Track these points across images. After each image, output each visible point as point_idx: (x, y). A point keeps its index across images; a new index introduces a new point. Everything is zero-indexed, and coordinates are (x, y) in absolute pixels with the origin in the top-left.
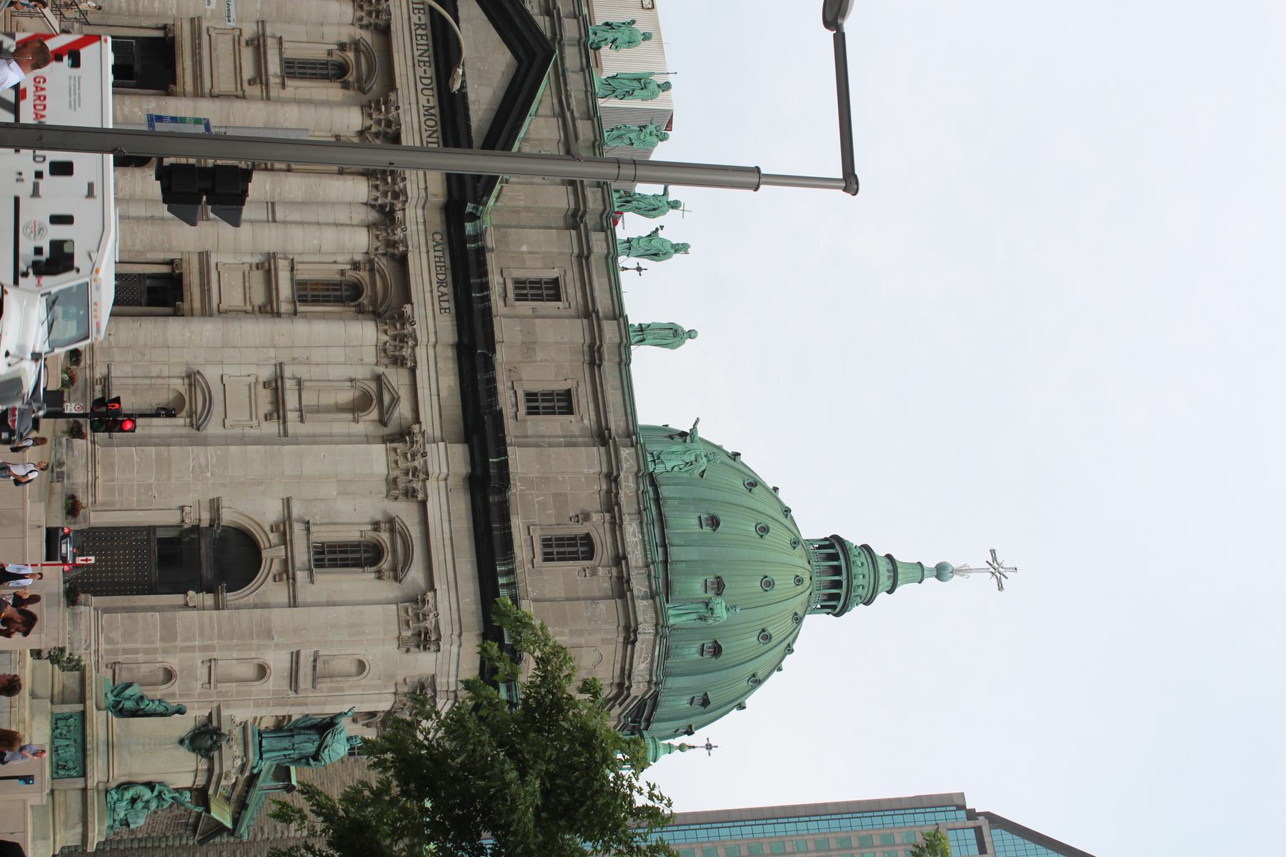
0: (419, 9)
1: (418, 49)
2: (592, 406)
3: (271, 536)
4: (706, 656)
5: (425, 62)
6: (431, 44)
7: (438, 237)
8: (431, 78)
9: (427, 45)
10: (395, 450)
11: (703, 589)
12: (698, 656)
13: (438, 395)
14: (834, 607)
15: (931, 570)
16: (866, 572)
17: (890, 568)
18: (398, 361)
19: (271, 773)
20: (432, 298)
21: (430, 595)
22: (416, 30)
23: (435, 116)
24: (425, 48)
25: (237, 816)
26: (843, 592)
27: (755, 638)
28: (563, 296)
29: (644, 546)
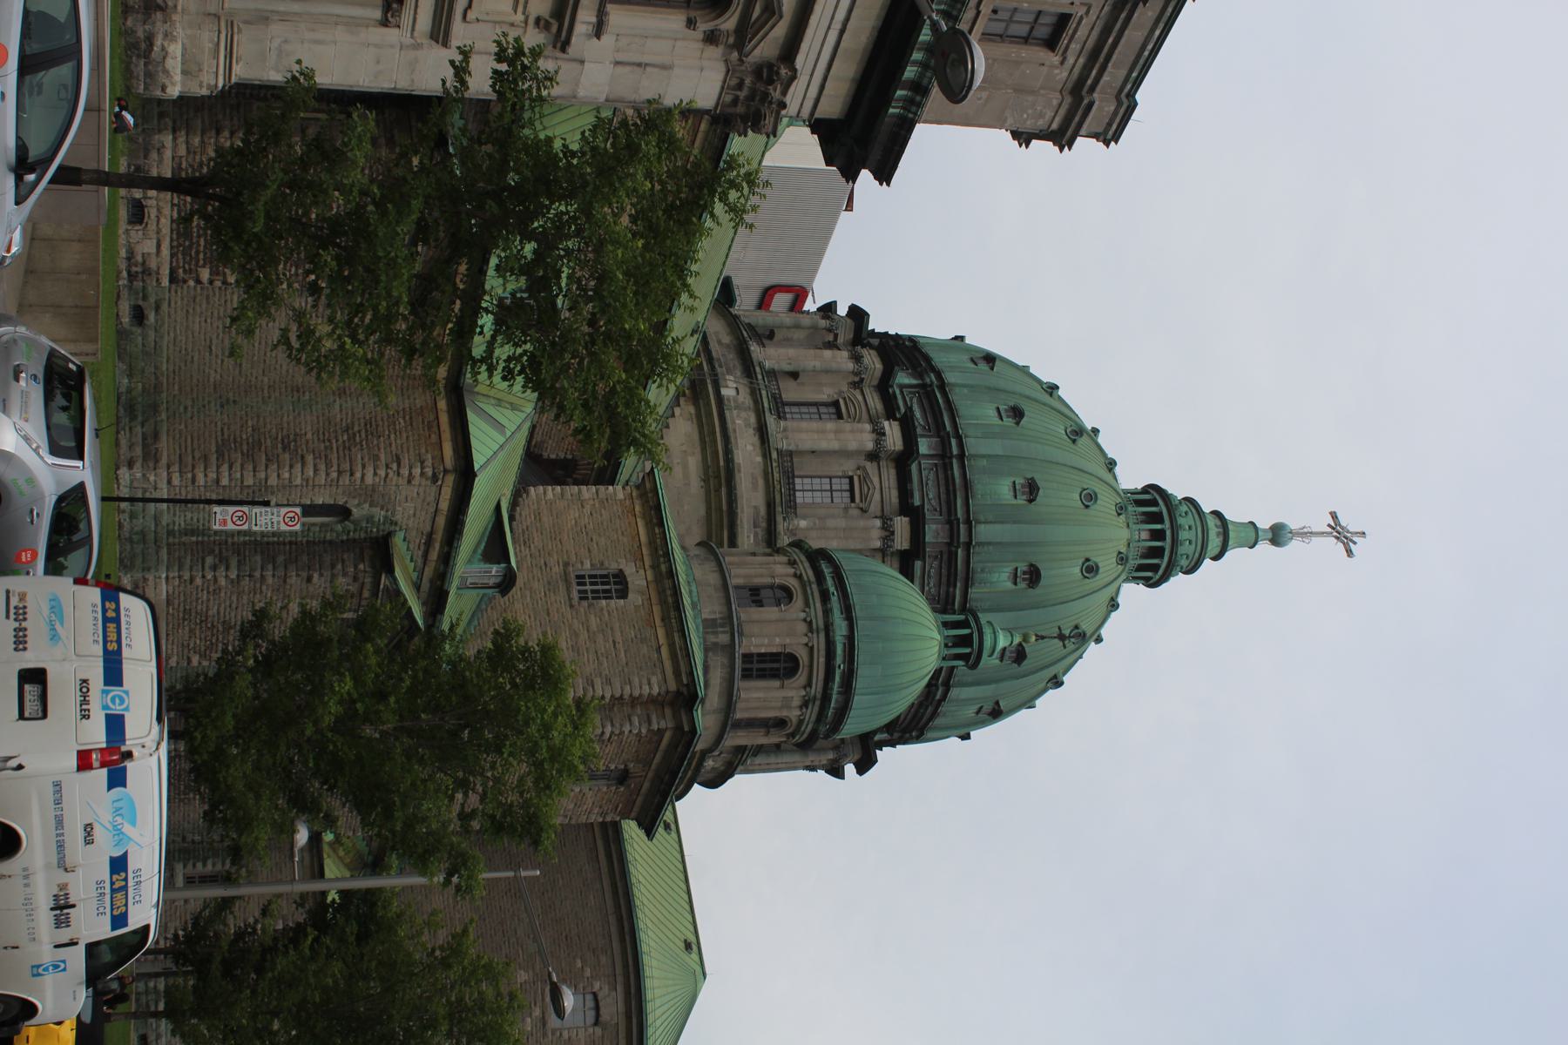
4: (1022, 585)
11: (1012, 493)
12: (1009, 585)
14: (1155, 568)
15: (1264, 531)
17: (1219, 523)
19: (480, 551)
25: (430, 622)
26: (1167, 544)
27: (1077, 570)
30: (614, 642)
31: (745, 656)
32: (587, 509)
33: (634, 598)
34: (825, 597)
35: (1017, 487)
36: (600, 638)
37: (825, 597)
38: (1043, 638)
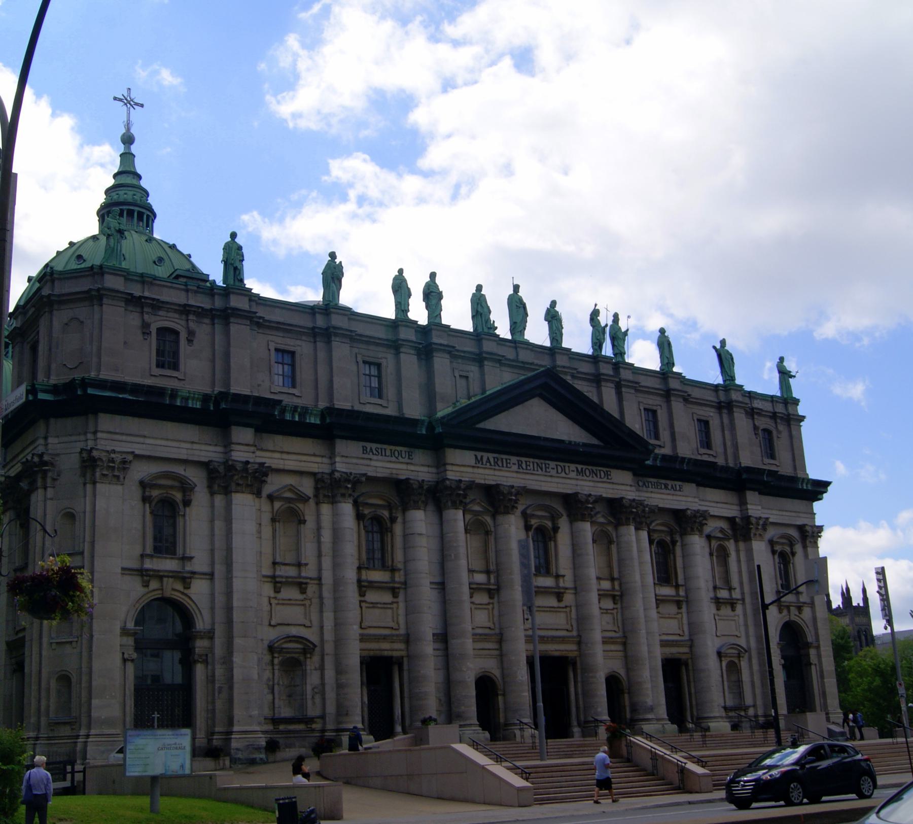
0: (507, 463)
1: (537, 471)
2: (704, 408)
3: (783, 614)
5: (546, 468)
6: (531, 460)
7: (641, 484)
8: (557, 465)
9: (533, 463)
10: (755, 534)
13: (717, 502)
16: (132, 193)
18: (702, 525)
20: (676, 495)
21: (808, 528)
22: (523, 468)
23: (582, 469)
24: (535, 464)
28: (654, 408)
29: (763, 399)
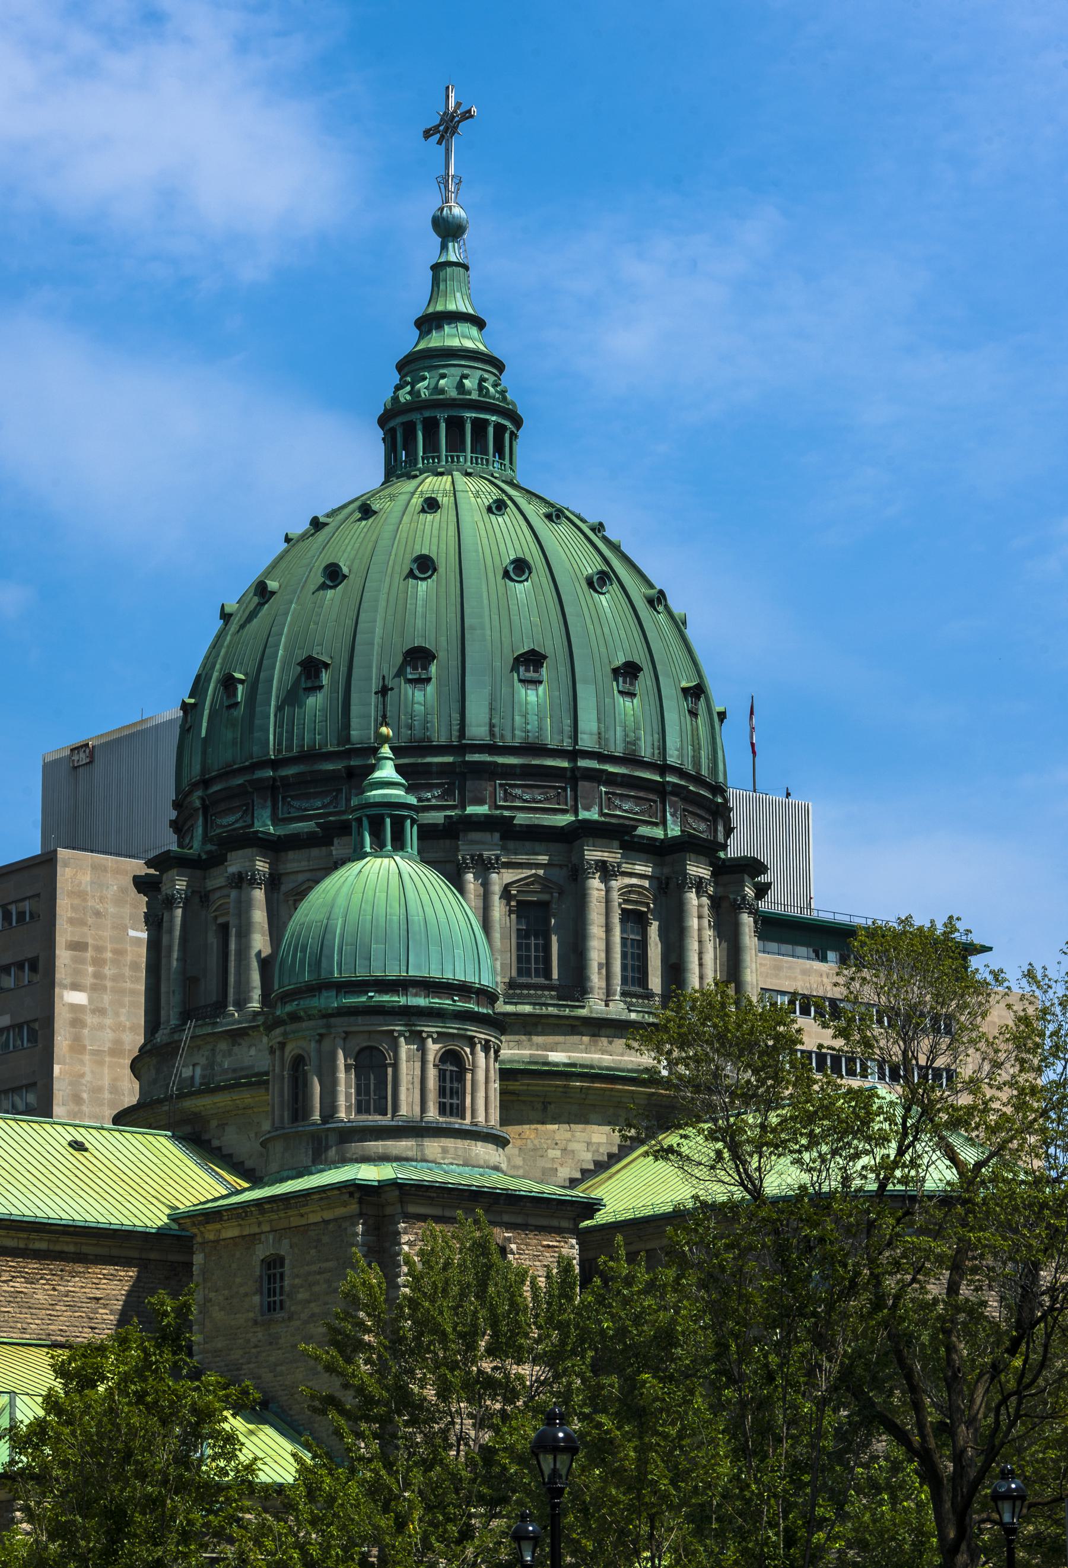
12: (430, 688)
26: (442, 416)
27: (422, 586)
30: (319, 1273)
31: (359, 1111)
32: (212, 1295)
33: (284, 1250)
34: (294, 1017)
35: (309, 685)
36: (316, 1289)
37: (294, 1017)
38: (384, 716)
